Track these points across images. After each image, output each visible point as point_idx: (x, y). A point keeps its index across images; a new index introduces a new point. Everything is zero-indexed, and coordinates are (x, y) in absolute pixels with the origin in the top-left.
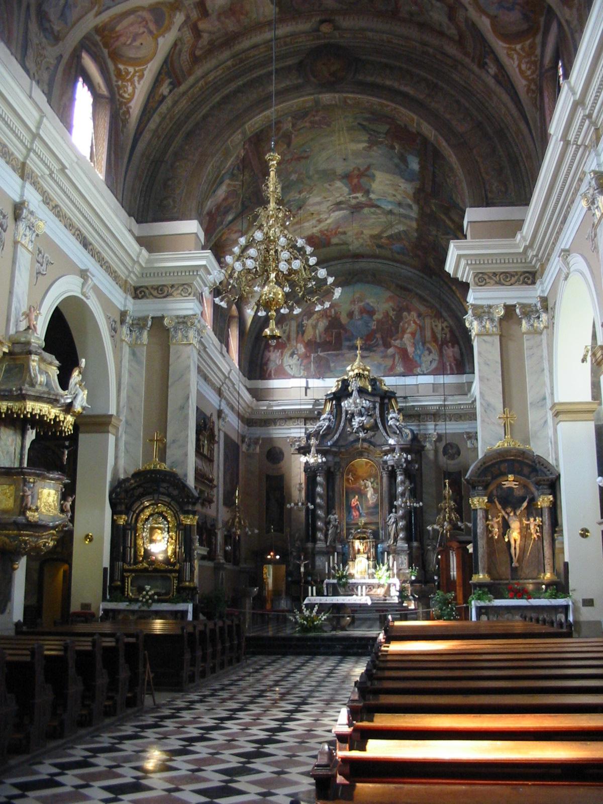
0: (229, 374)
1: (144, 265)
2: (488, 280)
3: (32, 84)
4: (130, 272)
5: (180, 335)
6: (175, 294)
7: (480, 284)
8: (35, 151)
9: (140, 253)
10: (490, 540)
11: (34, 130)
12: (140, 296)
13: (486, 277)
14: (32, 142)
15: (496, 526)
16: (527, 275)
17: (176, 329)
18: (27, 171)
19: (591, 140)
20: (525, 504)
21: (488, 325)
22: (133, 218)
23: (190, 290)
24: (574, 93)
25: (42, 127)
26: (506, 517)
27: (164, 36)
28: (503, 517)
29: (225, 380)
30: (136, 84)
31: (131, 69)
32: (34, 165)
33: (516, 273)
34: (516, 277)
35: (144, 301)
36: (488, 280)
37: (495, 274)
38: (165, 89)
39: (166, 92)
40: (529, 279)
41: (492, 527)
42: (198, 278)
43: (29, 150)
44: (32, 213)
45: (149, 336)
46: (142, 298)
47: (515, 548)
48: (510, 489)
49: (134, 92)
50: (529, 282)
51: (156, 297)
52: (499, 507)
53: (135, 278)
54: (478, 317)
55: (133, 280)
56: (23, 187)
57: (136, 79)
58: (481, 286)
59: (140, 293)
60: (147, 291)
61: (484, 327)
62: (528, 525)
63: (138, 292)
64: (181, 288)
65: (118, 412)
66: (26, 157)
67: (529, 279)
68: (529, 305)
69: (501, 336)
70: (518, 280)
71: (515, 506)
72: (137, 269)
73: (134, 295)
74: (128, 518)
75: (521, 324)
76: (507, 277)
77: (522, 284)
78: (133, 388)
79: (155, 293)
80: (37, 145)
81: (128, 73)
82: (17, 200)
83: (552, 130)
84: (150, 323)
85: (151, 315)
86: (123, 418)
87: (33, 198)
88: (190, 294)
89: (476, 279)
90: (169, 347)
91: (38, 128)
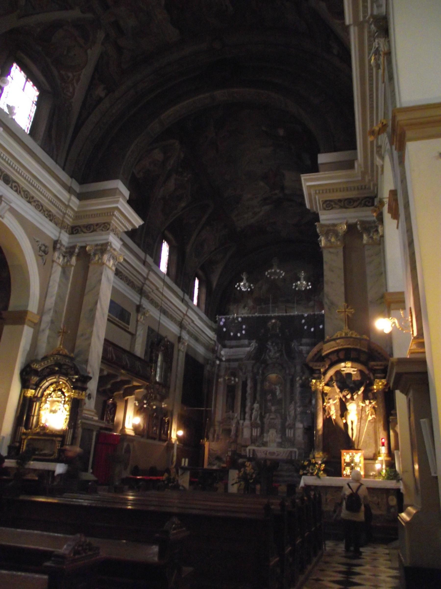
0: (187, 312)
1: (76, 209)
2: (334, 206)
4: (65, 214)
5: (97, 258)
6: (98, 230)
7: (327, 209)
9: (69, 200)
10: (328, 421)
12: (75, 232)
13: (332, 203)
15: (333, 408)
16: (368, 199)
17: (95, 254)
20: (362, 389)
21: (333, 240)
22: (74, 180)
23: (108, 226)
26: (344, 400)
27: (91, 49)
28: (340, 399)
29: (184, 316)
30: (75, 84)
31: (70, 74)
33: (358, 199)
34: (358, 202)
35: (78, 235)
36: (334, 206)
37: (340, 201)
38: (100, 91)
39: (103, 94)
40: (369, 202)
41: (329, 408)
42: (114, 218)
45: (77, 260)
46: (76, 233)
47: (352, 429)
48: (349, 375)
49: (74, 90)
50: (370, 204)
51: (84, 233)
52: (338, 390)
53: (71, 220)
54: (327, 234)
55: (69, 221)
57: (75, 81)
58: (328, 210)
59: (75, 230)
60: (80, 229)
61: (330, 241)
62: (363, 409)
63: (74, 230)
64: (102, 226)
65: (41, 312)
67: (369, 202)
68: (369, 222)
69: (344, 248)
70: (360, 203)
71: (353, 390)
72: (71, 213)
73: (70, 232)
74: (36, 392)
75: (362, 238)
76: (350, 202)
77: (363, 207)
78: (60, 297)
79: (85, 230)
81: (68, 77)
84: (77, 250)
85: (79, 245)
86: (47, 318)
88: (108, 229)
89: (325, 205)
90: (88, 267)
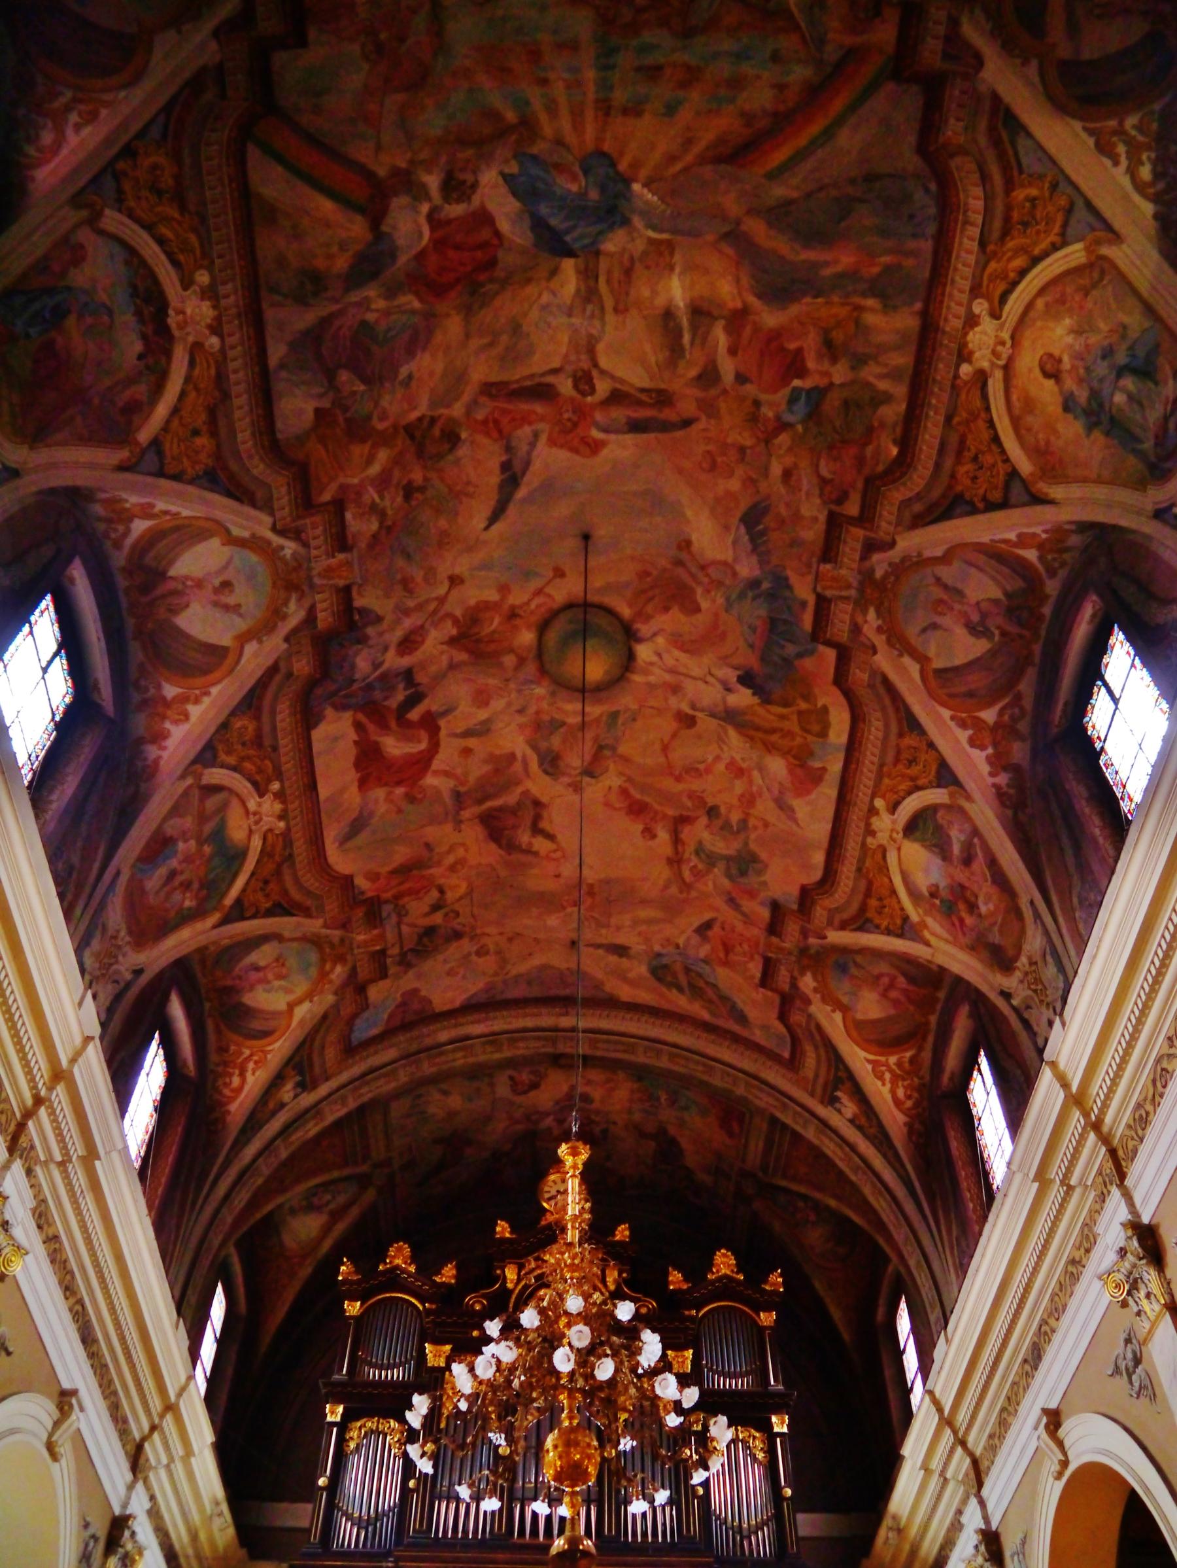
3: (178, 1321)
8: (163, 1433)
11: (173, 1398)
14: (162, 1416)
18: (142, 1461)
19: (967, 1475)
24: (940, 1410)
25: (185, 1395)
32: (154, 1451)
43: (153, 1428)
44: (133, 1534)
56: (131, 1487)
66: (144, 1439)
80: (169, 1422)
82: (117, 1511)
83: (907, 1450)
87: (139, 1505)
91: (179, 1395)
